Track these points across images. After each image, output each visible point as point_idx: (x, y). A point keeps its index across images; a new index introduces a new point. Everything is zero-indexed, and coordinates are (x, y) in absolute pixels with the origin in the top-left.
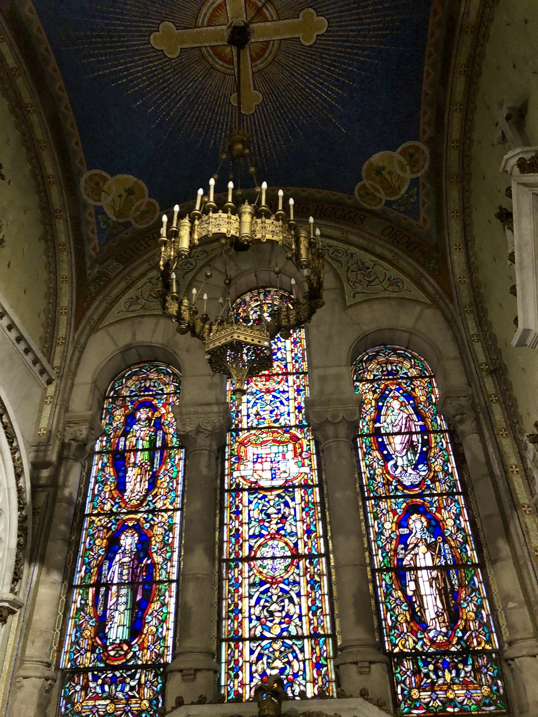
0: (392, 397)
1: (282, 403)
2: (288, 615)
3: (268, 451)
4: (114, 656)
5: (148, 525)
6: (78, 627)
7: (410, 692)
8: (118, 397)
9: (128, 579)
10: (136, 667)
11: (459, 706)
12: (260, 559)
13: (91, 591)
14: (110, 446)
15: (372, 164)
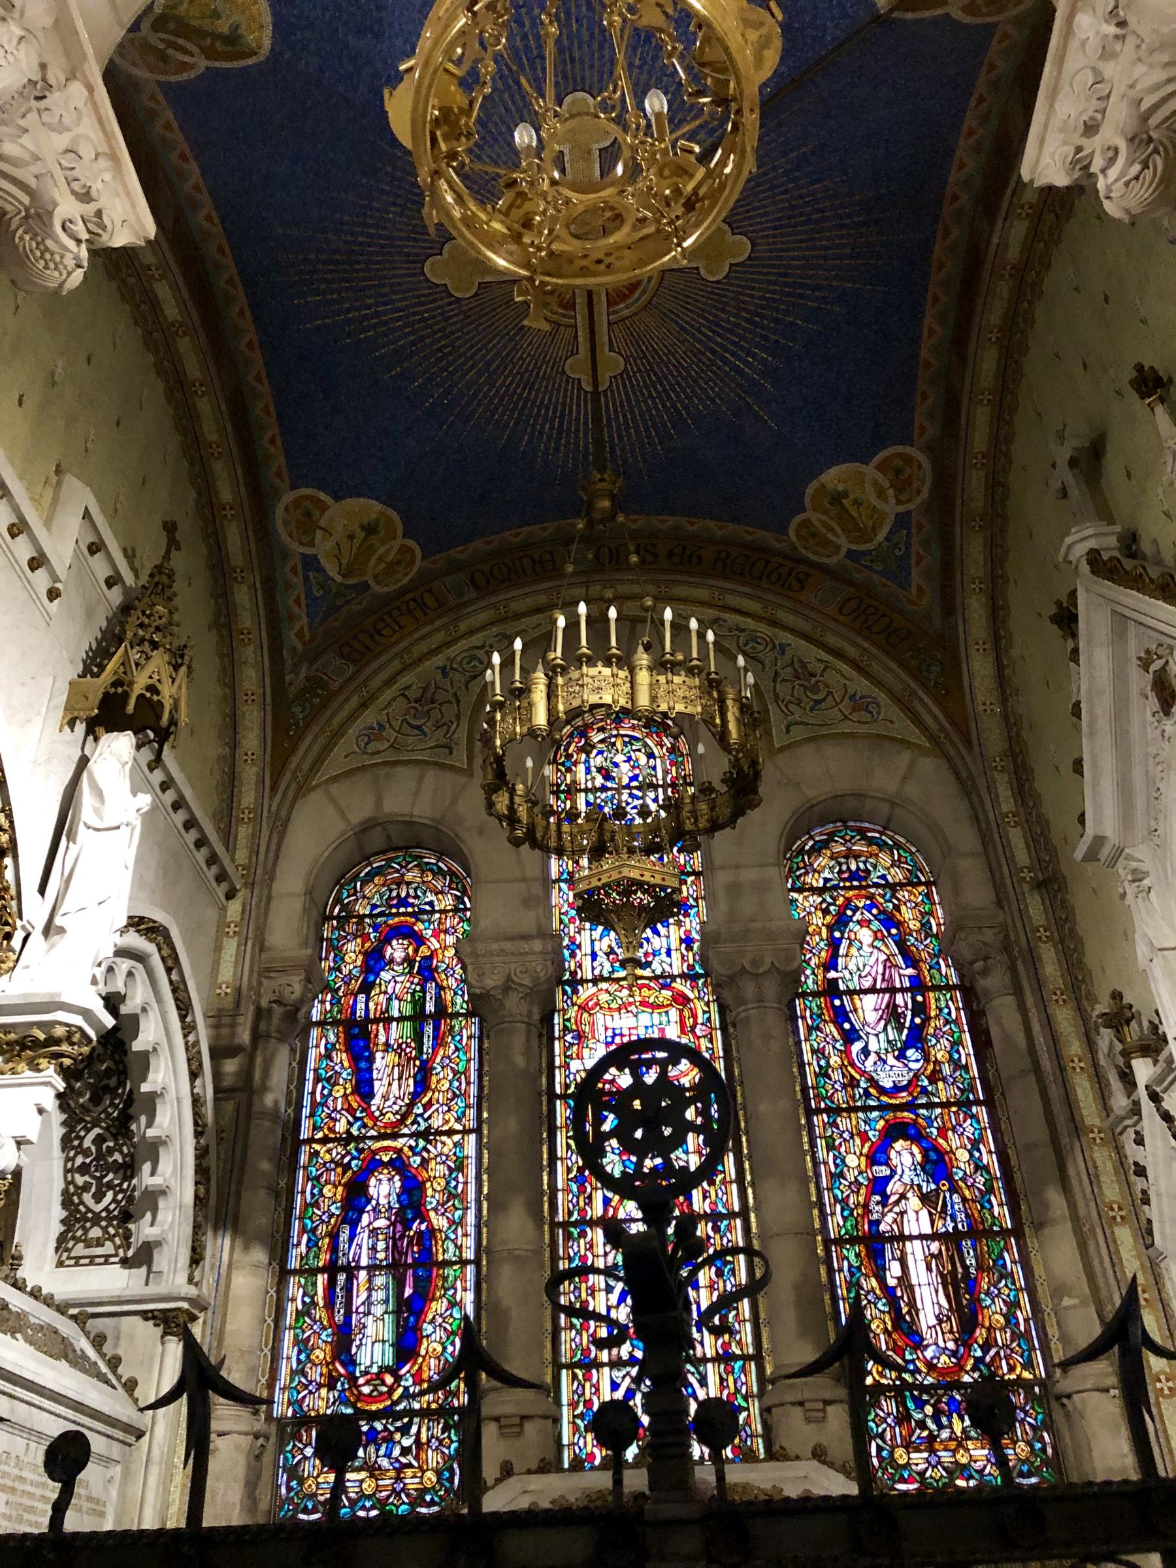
0: (858, 922)
3: (632, 1022)
4: (370, 1395)
5: (418, 1159)
6: (302, 1344)
7: (891, 1453)
8: (349, 916)
10: (411, 1413)
11: (976, 1476)
13: (321, 1279)
14: (340, 1012)
15: (823, 486)
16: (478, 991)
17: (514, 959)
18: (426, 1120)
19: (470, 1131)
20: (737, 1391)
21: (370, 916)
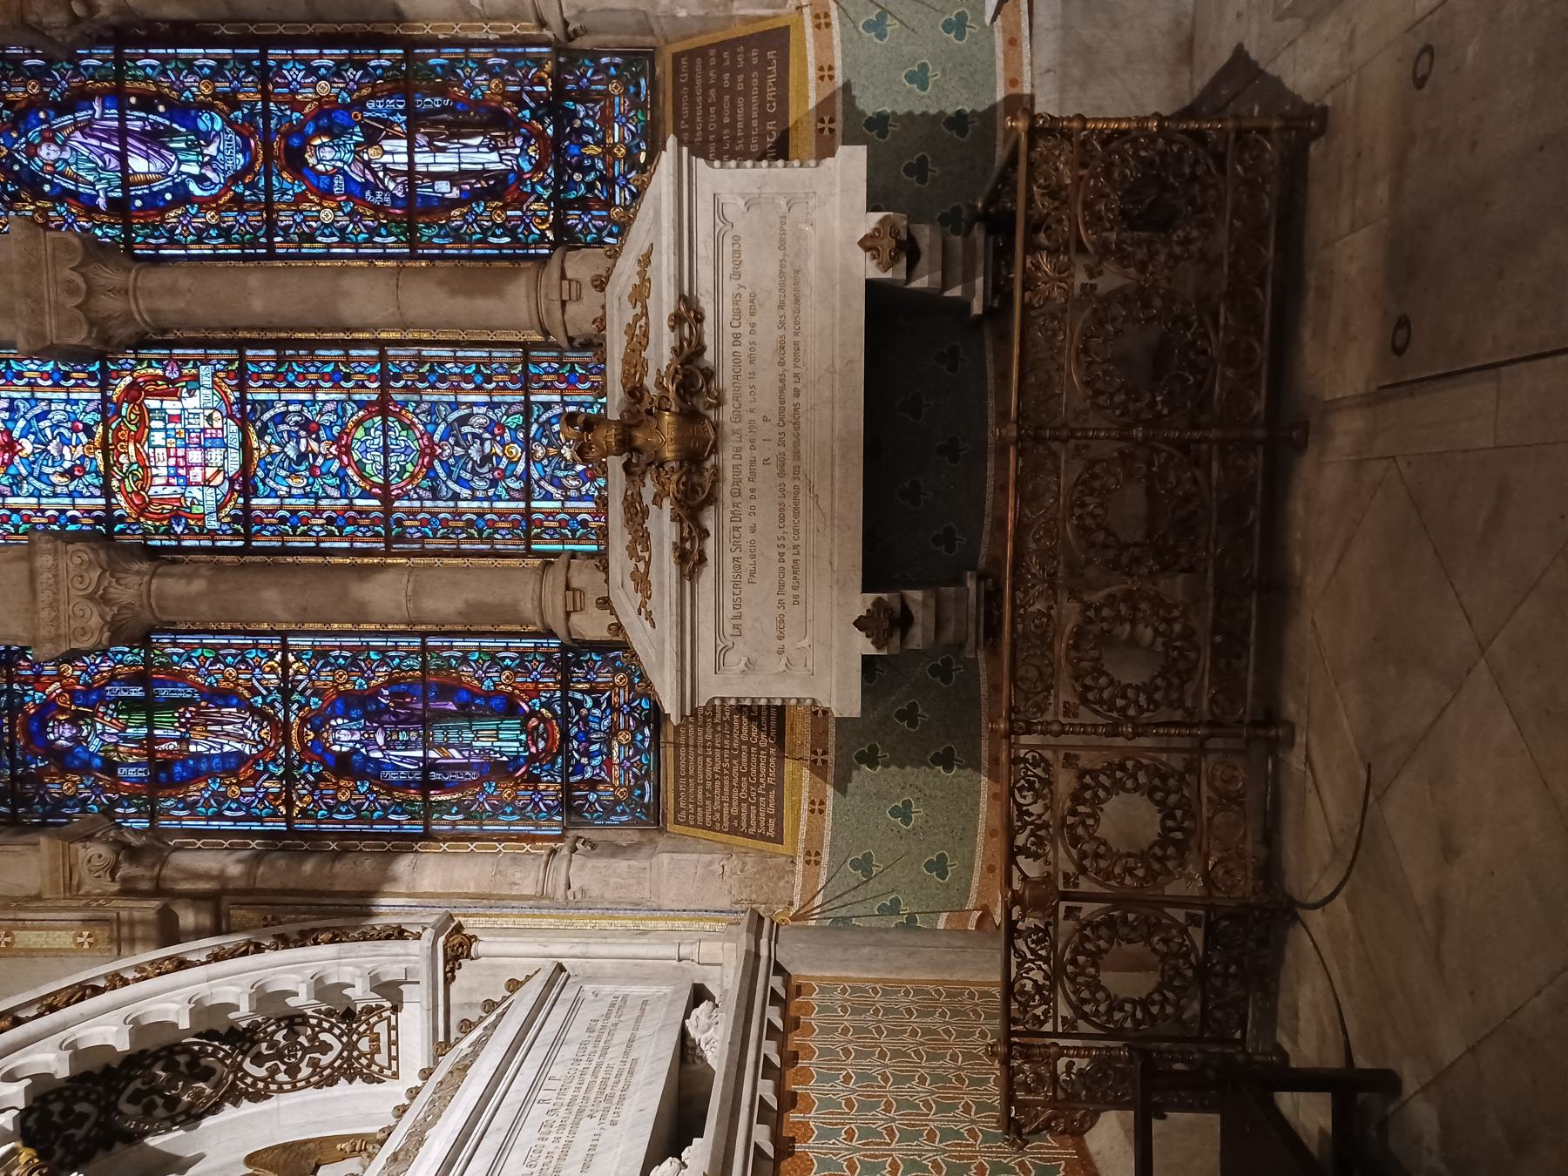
1: (43, 416)
7: (615, 223)
9: (416, 730)
10: (565, 699)
11: (637, 140)
12: (386, 477)
16: (106, 635)
17: (63, 591)
18: (270, 692)
19: (284, 642)
20: (556, 372)
21: (13, 768)
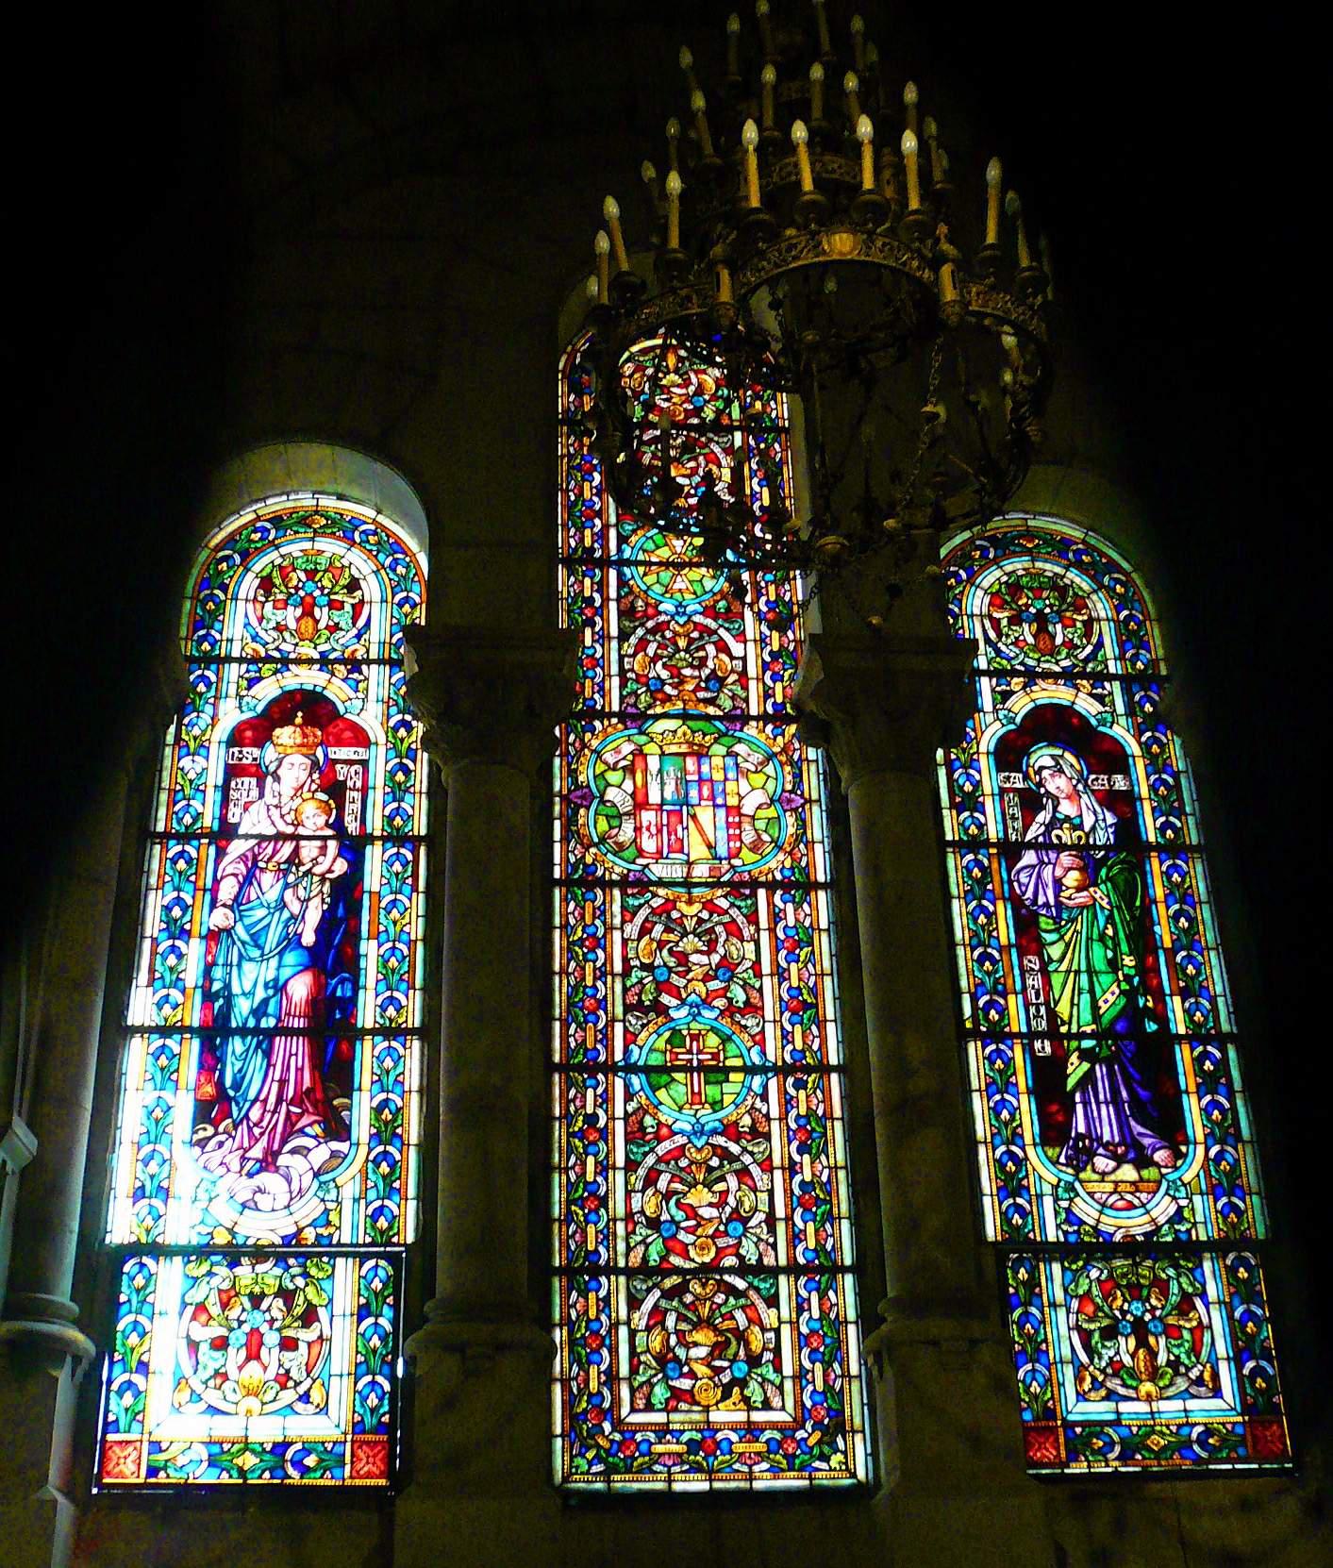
2: (736, 1216)
